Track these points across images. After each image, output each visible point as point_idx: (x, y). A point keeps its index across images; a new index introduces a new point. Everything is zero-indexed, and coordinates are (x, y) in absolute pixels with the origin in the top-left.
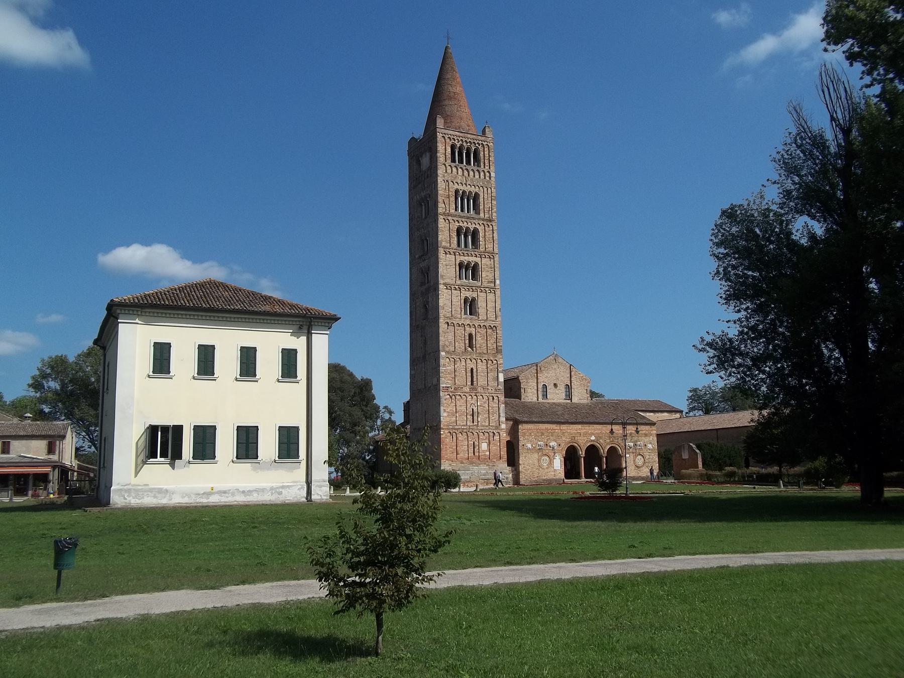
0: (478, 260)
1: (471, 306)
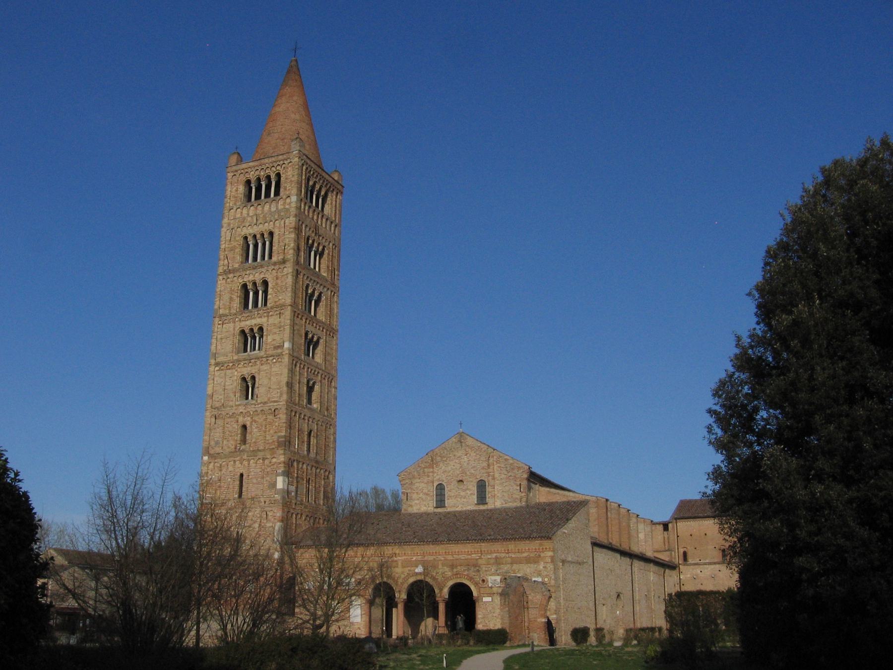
0: (263, 321)
1: (248, 386)
